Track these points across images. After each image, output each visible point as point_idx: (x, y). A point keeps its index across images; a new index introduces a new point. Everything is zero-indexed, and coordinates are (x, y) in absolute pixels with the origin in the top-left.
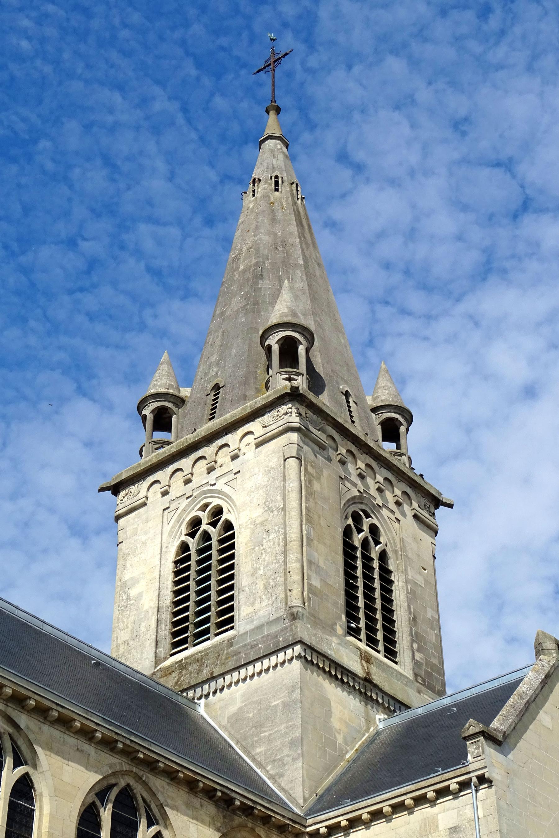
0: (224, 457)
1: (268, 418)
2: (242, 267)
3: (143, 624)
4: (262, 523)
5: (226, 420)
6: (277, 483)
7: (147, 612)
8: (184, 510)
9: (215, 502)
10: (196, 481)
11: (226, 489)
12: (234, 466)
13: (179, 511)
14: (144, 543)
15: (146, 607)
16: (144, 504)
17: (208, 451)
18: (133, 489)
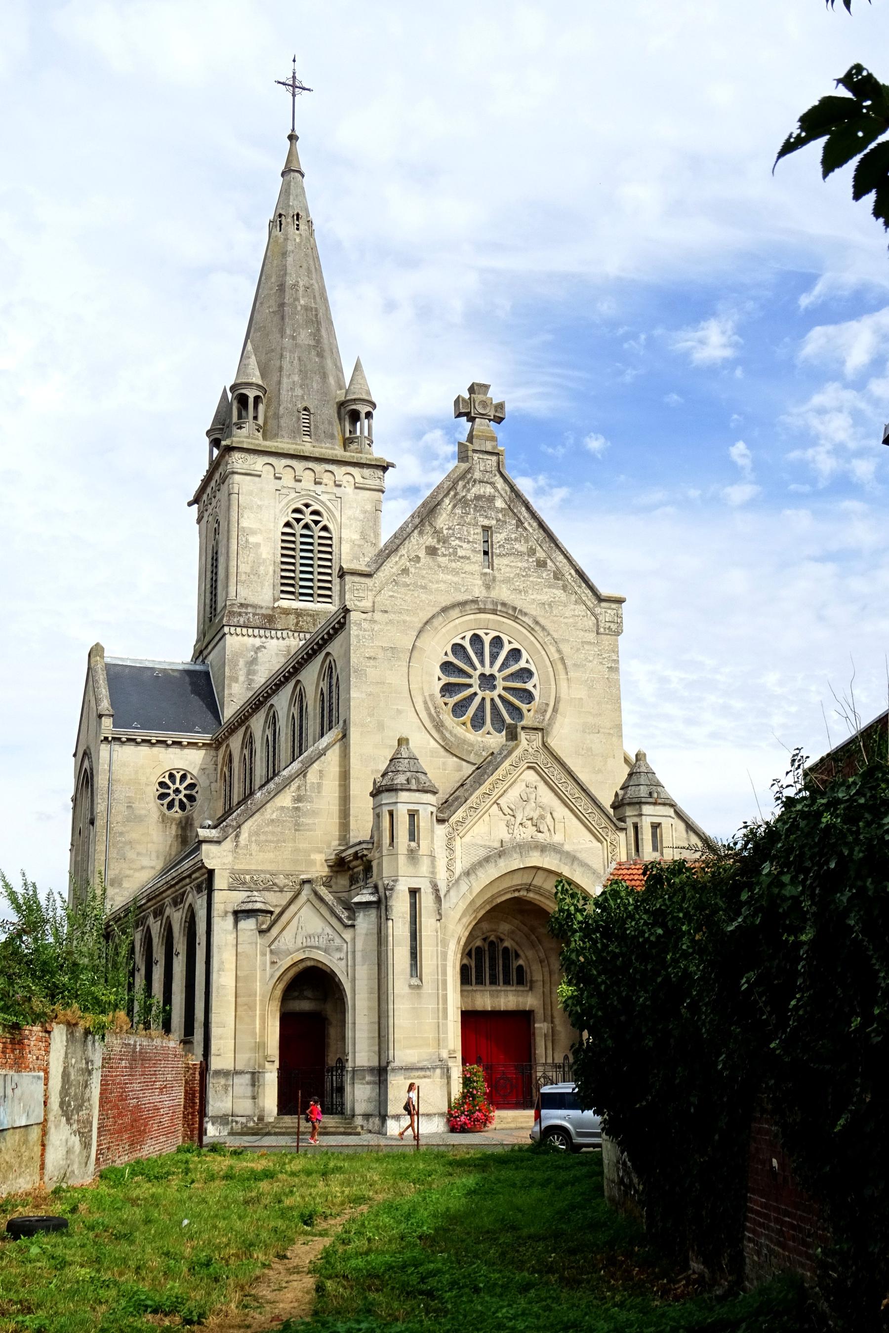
0: (327, 478)
1: (367, 472)
2: (302, 302)
3: (262, 568)
4: (359, 546)
5: (336, 456)
6: (371, 524)
7: (264, 560)
8: (293, 499)
9: (316, 507)
10: (303, 484)
11: (328, 504)
12: (336, 490)
13: (289, 498)
14: (260, 507)
15: (264, 556)
16: (260, 476)
17: (319, 468)
18: (251, 458)
